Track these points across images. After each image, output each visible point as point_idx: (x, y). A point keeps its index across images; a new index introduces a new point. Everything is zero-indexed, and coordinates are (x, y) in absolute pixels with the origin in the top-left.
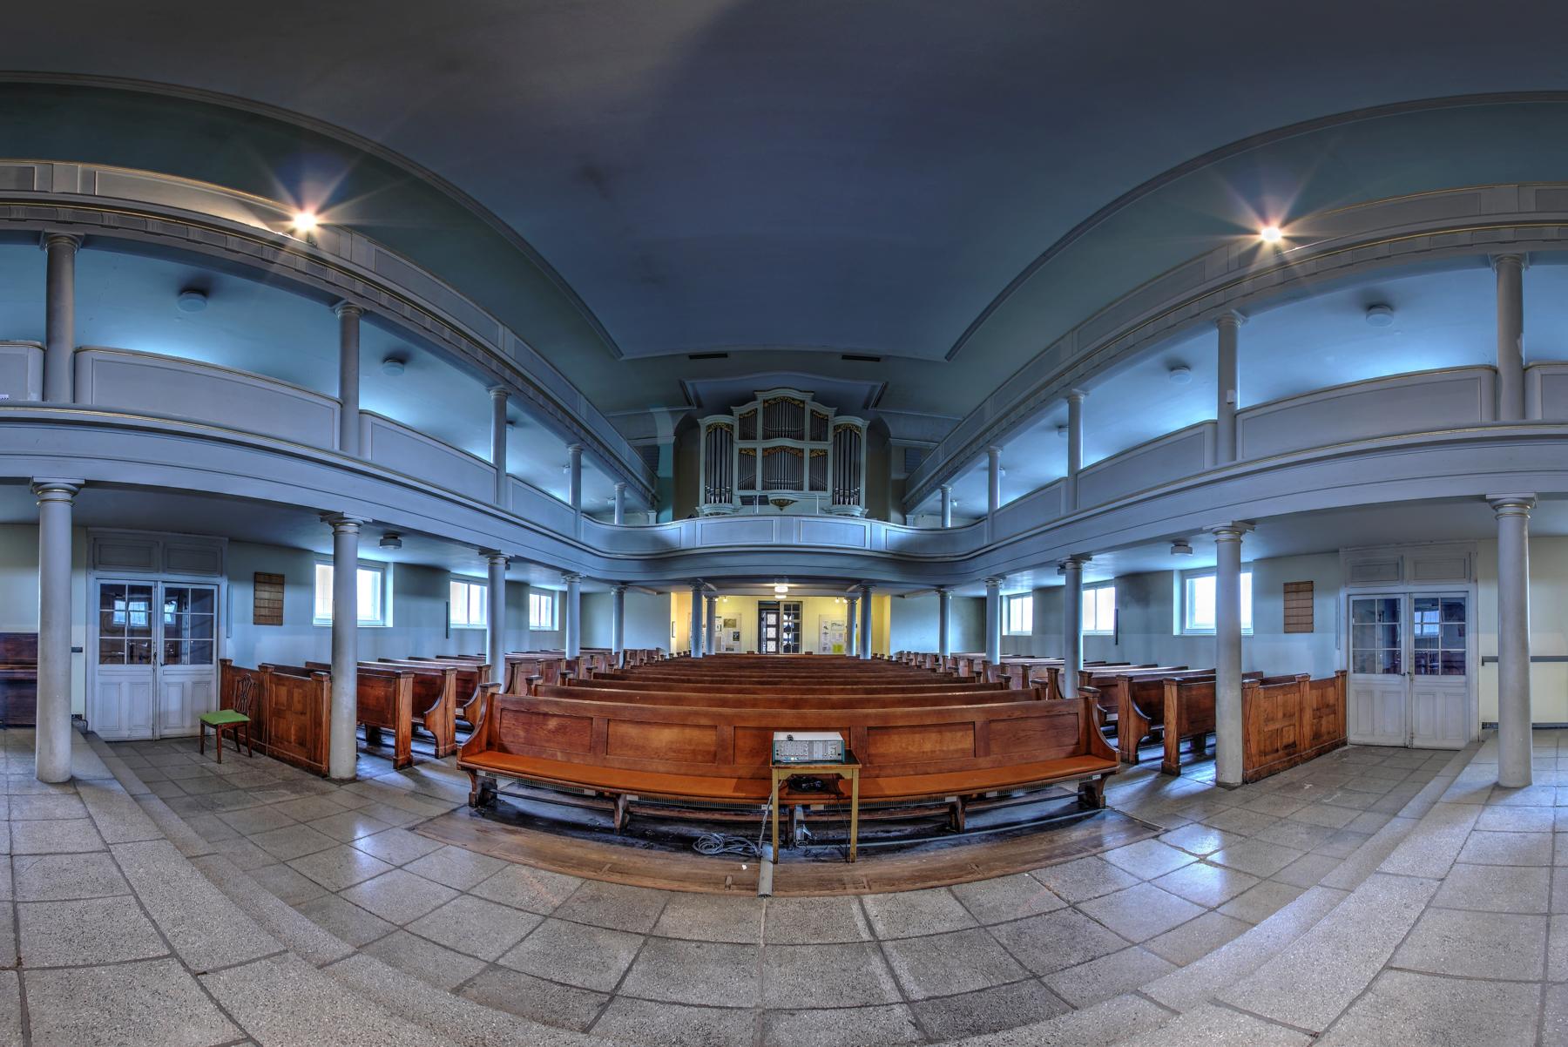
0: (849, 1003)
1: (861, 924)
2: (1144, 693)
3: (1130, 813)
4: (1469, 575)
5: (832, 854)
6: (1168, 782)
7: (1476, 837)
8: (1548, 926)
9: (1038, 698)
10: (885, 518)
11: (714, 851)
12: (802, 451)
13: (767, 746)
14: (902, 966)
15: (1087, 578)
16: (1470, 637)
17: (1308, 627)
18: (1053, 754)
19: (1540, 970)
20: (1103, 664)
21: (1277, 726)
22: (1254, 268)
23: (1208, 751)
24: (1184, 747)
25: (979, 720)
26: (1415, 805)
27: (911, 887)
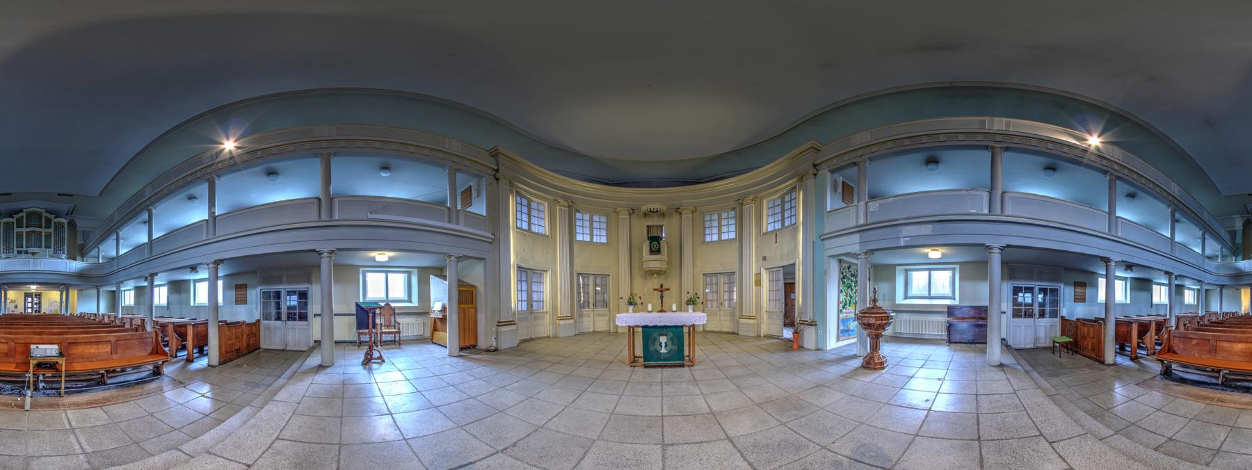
0: (61, 454)
1: (66, 422)
2: (179, 329)
3: (174, 377)
4: (309, 281)
5: (54, 394)
6: (188, 365)
7: (312, 386)
8: (341, 422)
9: (137, 331)
10: (75, 259)
11: (7, 393)
12: (41, 232)
13: (27, 352)
14: (82, 440)
15: (156, 283)
16: (309, 306)
17: (245, 302)
18: (143, 353)
19: (338, 439)
20: (162, 317)
21: (233, 341)
22: (219, 159)
23: (205, 352)
24: (195, 351)
25: (113, 340)
26: (288, 373)
27: (86, 407)
